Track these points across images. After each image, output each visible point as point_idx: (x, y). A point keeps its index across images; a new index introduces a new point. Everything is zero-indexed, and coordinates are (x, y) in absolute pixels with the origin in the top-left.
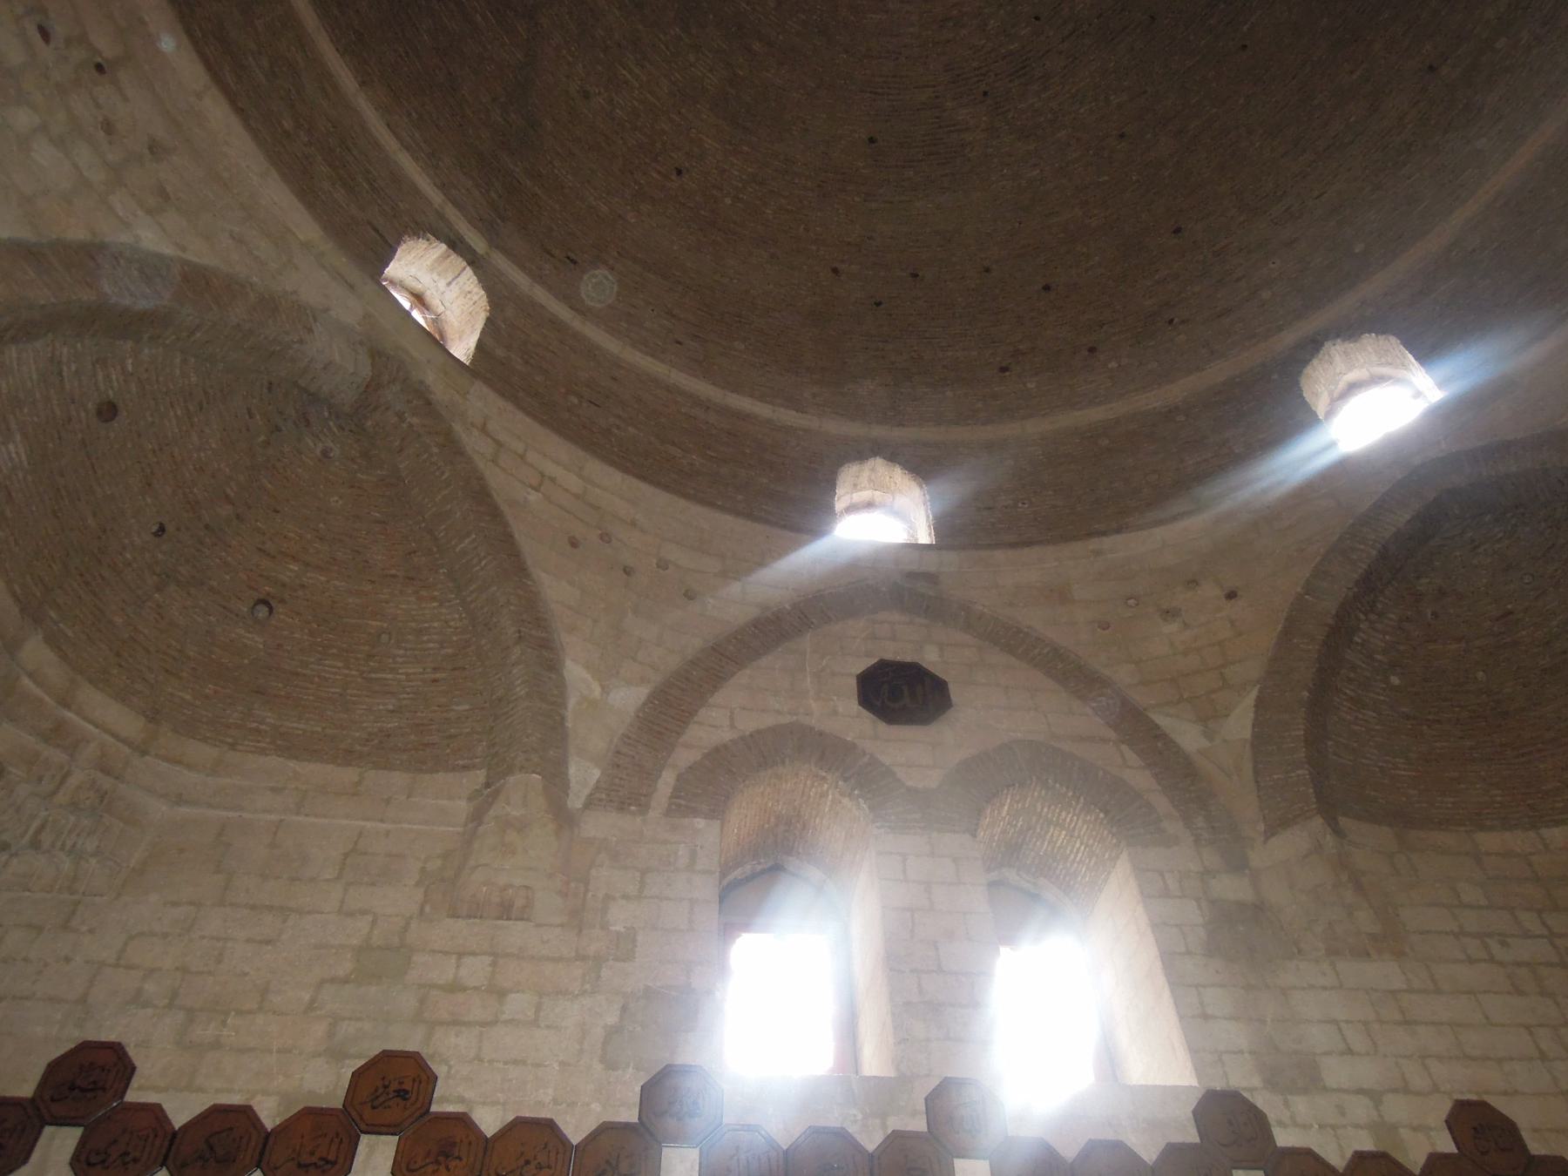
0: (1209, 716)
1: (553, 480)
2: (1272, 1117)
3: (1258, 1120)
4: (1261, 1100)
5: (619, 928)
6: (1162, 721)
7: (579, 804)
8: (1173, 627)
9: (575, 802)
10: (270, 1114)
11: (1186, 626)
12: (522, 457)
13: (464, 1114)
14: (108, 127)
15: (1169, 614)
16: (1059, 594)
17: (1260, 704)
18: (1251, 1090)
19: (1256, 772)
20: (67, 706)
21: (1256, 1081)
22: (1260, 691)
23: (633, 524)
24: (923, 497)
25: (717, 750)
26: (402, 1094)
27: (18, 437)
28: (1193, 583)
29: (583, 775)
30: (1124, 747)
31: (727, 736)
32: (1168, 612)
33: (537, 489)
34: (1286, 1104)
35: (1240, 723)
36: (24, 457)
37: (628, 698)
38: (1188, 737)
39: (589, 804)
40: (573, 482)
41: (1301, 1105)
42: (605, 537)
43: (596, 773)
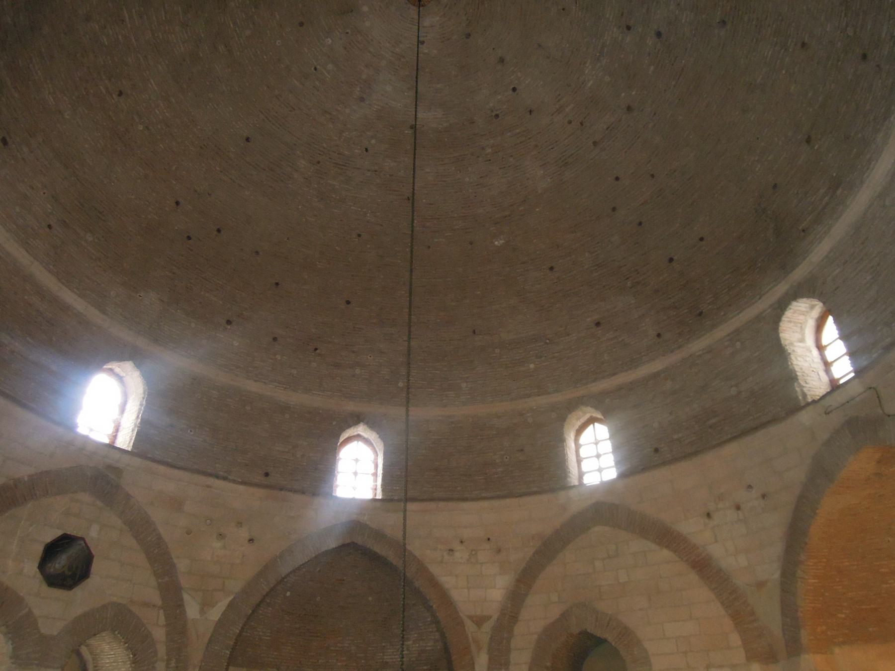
0: (206, 605)
6: (186, 597)
8: (217, 545)
15: (221, 536)
16: (176, 504)
17: (230, 605)
19: (210, 641)
22: (234, 598)
24: (142, 399)
28: (240, 524)
30: (162, 611)
32: (221, 535)
35: (215, 614)
38: (192, 610)
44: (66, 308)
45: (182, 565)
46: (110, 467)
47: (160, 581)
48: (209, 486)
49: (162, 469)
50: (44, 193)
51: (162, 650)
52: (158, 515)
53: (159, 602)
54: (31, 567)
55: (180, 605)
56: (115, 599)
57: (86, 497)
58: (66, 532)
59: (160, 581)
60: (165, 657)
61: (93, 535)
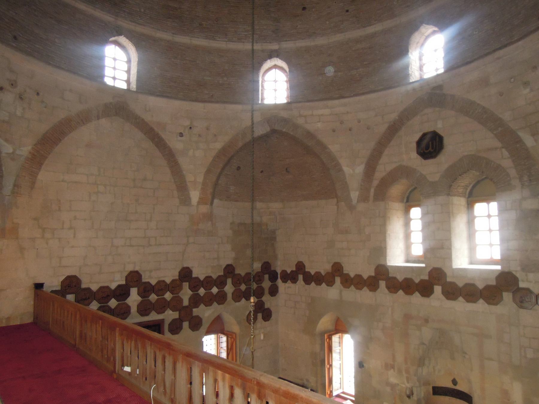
1: (322, 115)
2: (520, 279)
3: (515, 280)
4: (518, 275)
5: (367, 233)
6: (521, 134)
7: (356, 202)
8: (527, 91)
9: (355, 201)
10: (323, 273)
11: (532, 90)
12: (312, 115)
13: (348, 274)
14: (200, 136)
15: (526, 84)
16: (484, 82)
18: (516, 271)
20: (269, 209)
21: (519, 268)
23: (348, 113)
25: (382, 179)
26: (339, 270)
27: (231, 187)
29: (354, 195)
30: (504, 150)
31: (384, 174)
32: (525, 83)
33: (319, 122)
34: (526, 275)
36: (234, 187)
37: (360, 169)
39: (358, 202)
40: (327, 111)
41: (531, 276)
42: (342, 122)
43: (357, 193)
44: (373, 36)
45: (507, 116)
46: (434, 88)
47: (495, 132)
48: (498, 58)
49: (462, 69)
50: (335, 2)
51: (513, 172)
52: (475, 97)
53: (499, 144)
54: (414, 155)
55: (519, 141)
56: (466, 154)
57: (428, 111)
58: (423, 132)
59: (495, 132)
60: (517, 176)
61: (439, 127)
